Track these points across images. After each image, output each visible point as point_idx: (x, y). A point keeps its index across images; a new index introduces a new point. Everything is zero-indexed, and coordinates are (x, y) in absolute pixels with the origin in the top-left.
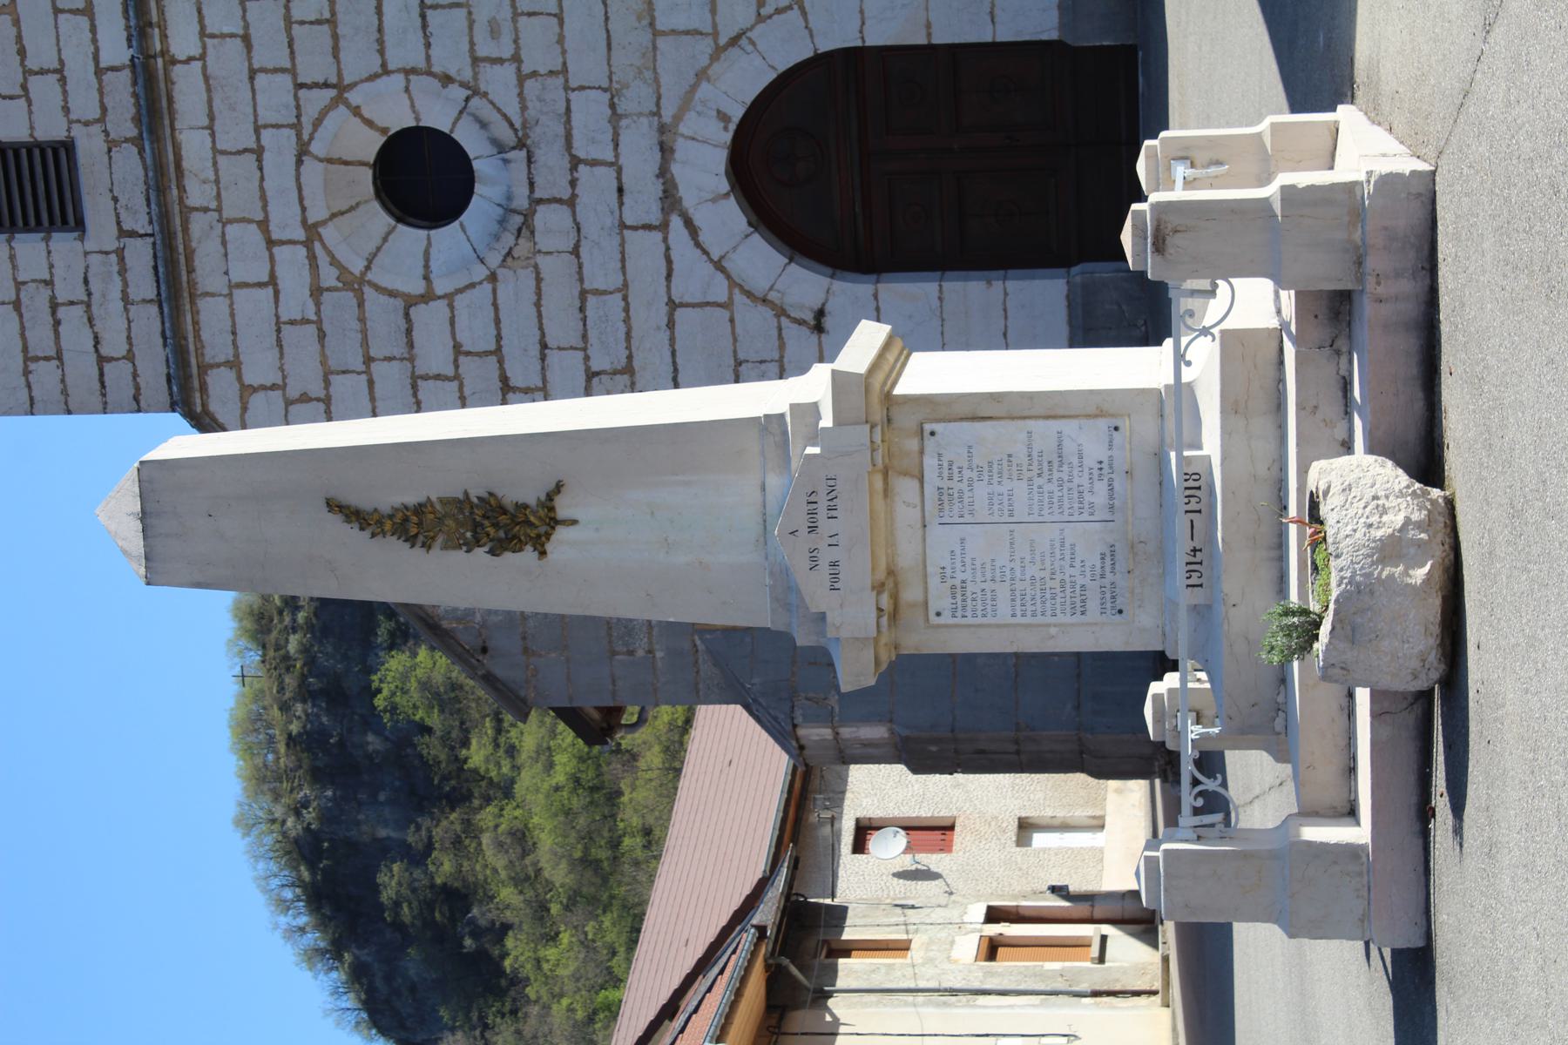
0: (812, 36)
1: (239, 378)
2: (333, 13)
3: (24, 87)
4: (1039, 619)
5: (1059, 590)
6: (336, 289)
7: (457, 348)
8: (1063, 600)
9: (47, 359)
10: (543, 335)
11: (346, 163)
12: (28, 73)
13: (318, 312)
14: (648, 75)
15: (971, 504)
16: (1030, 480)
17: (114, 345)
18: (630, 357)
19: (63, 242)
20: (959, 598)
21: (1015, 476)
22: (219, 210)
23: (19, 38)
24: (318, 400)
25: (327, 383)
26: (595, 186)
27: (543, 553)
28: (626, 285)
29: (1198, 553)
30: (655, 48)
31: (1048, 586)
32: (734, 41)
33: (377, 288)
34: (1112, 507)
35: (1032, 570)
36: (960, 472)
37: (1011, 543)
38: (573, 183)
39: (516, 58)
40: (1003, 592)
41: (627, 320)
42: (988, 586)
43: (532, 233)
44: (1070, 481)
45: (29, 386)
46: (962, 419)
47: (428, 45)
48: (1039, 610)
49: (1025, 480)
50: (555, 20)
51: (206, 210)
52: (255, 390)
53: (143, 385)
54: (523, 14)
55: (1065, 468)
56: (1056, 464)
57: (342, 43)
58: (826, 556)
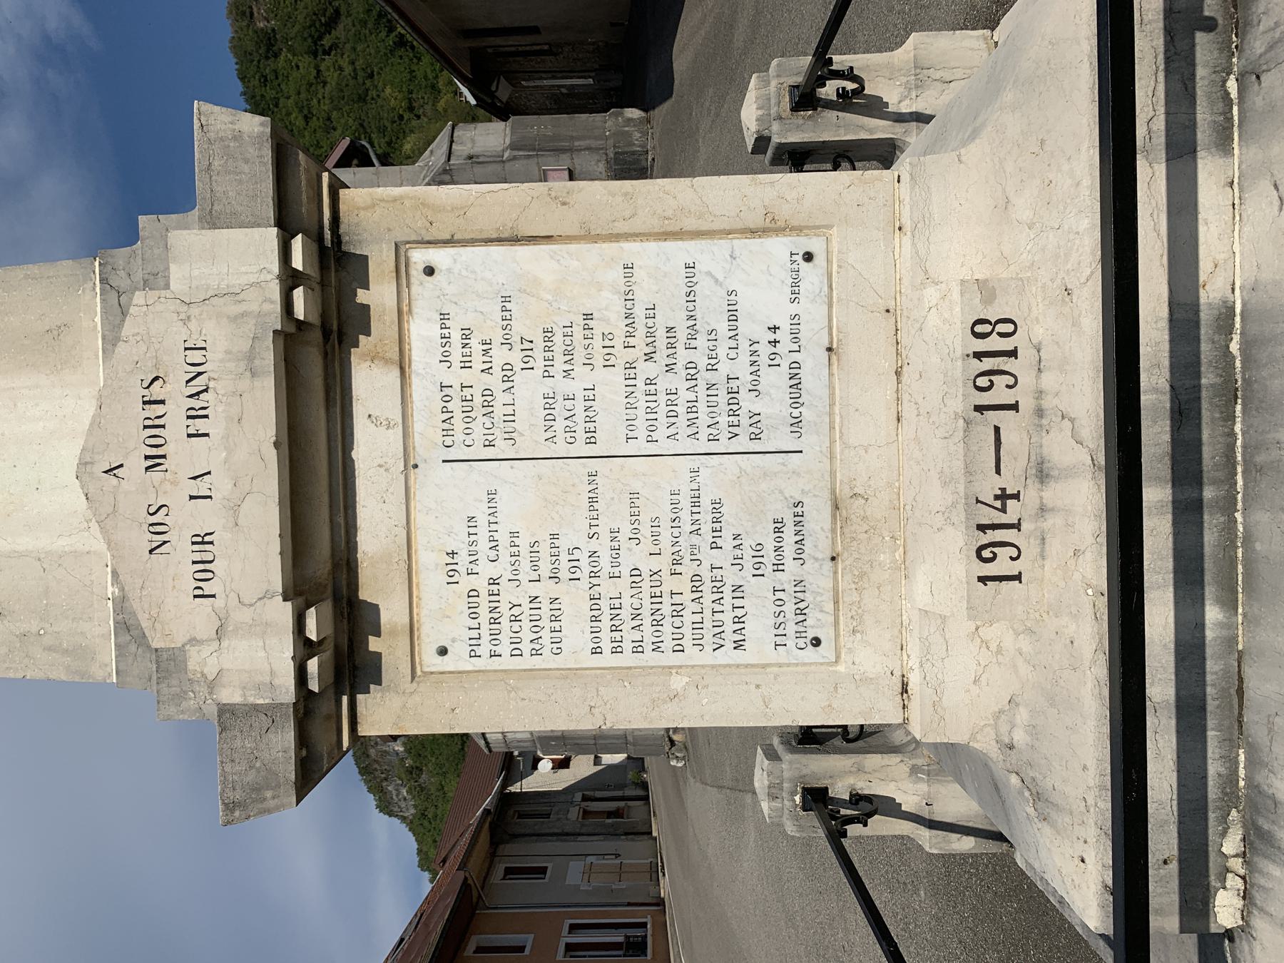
4: (649, 658)
5: (689, 596)
8: (697, 618)
15: (510, 418)
16: (630, 366)
20: (484, 616)
21: (598, 361)
29: (1010, 503)
31: (666, 589)
34: (797, 422)
35: (634, 556)
36: (486, 352)
37: (592, 500)
40: (575, 601)
42: (545, 590)
44: (712, 369)
46: (488, 241)
48: (649, 639)
55: (701, 342)
56: (682, 334)
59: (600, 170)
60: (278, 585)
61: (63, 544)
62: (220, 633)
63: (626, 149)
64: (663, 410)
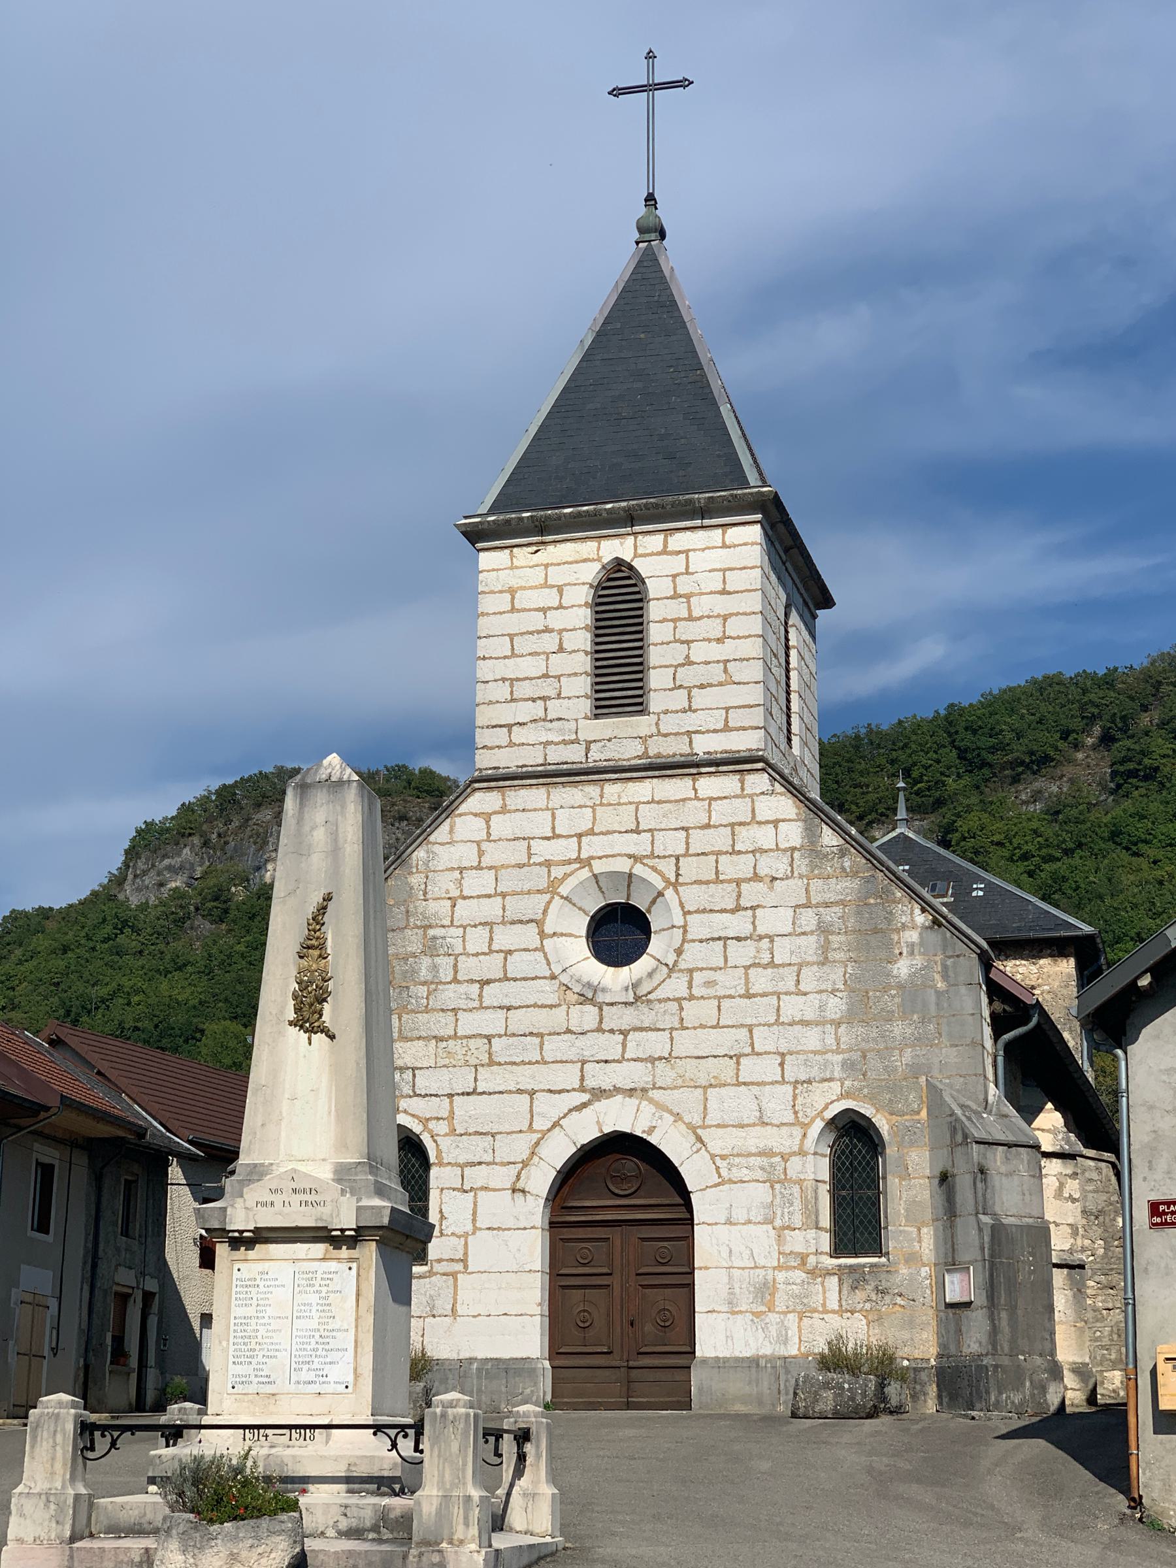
0: (701, 1190)
1: (495, 813)
2: (722, 882)
3: (681, 687)
4: (232, 1334)
5: (249, 1347)
6: (549, 876)
7: (510, 952)
9: (512, 692)
10: (516, 1008)
11: (629, 886)
12: (689, 689)
13: (535, 864)
14: (679, 1082)
16: (319, 1330)
17: (519, 735)
18: (500, 1064)
19: (586, 706)
21: (321, 1320)
22: (601, 804)
23: (711, 685)
24: (480, 862)
25: (490, 868)
26: (610, 1046)
27: (291, 1023)
28: (546, 1063)
30: (696, 1087)
32: (699, 1139)
33: (549, 903)
34: (299, 1383)
38: (612, 1031)
39: (691, 998)
40: (250, 1311)
41: (523, 1063)
42: (254, 1302)
43: (581, 1004)
45: (495, 681)
46: (358, 1286)
47: (701, 941)
48: (238, 1334)
49: (318, 1327)
50: (715, 1023)
51: (602, 796)
52: (487, 822)
53: (493, 751)
54: (719, 1002)
55: (324, 1353)
56: (327, 1347)
57: (704, 886)
58: (278, 1199)
59: (972, 1345)
60: (259, 1226)
61: (282, 1147)
62: (246, 1208)
63: (991, 1381)
64: (305, 1340)
